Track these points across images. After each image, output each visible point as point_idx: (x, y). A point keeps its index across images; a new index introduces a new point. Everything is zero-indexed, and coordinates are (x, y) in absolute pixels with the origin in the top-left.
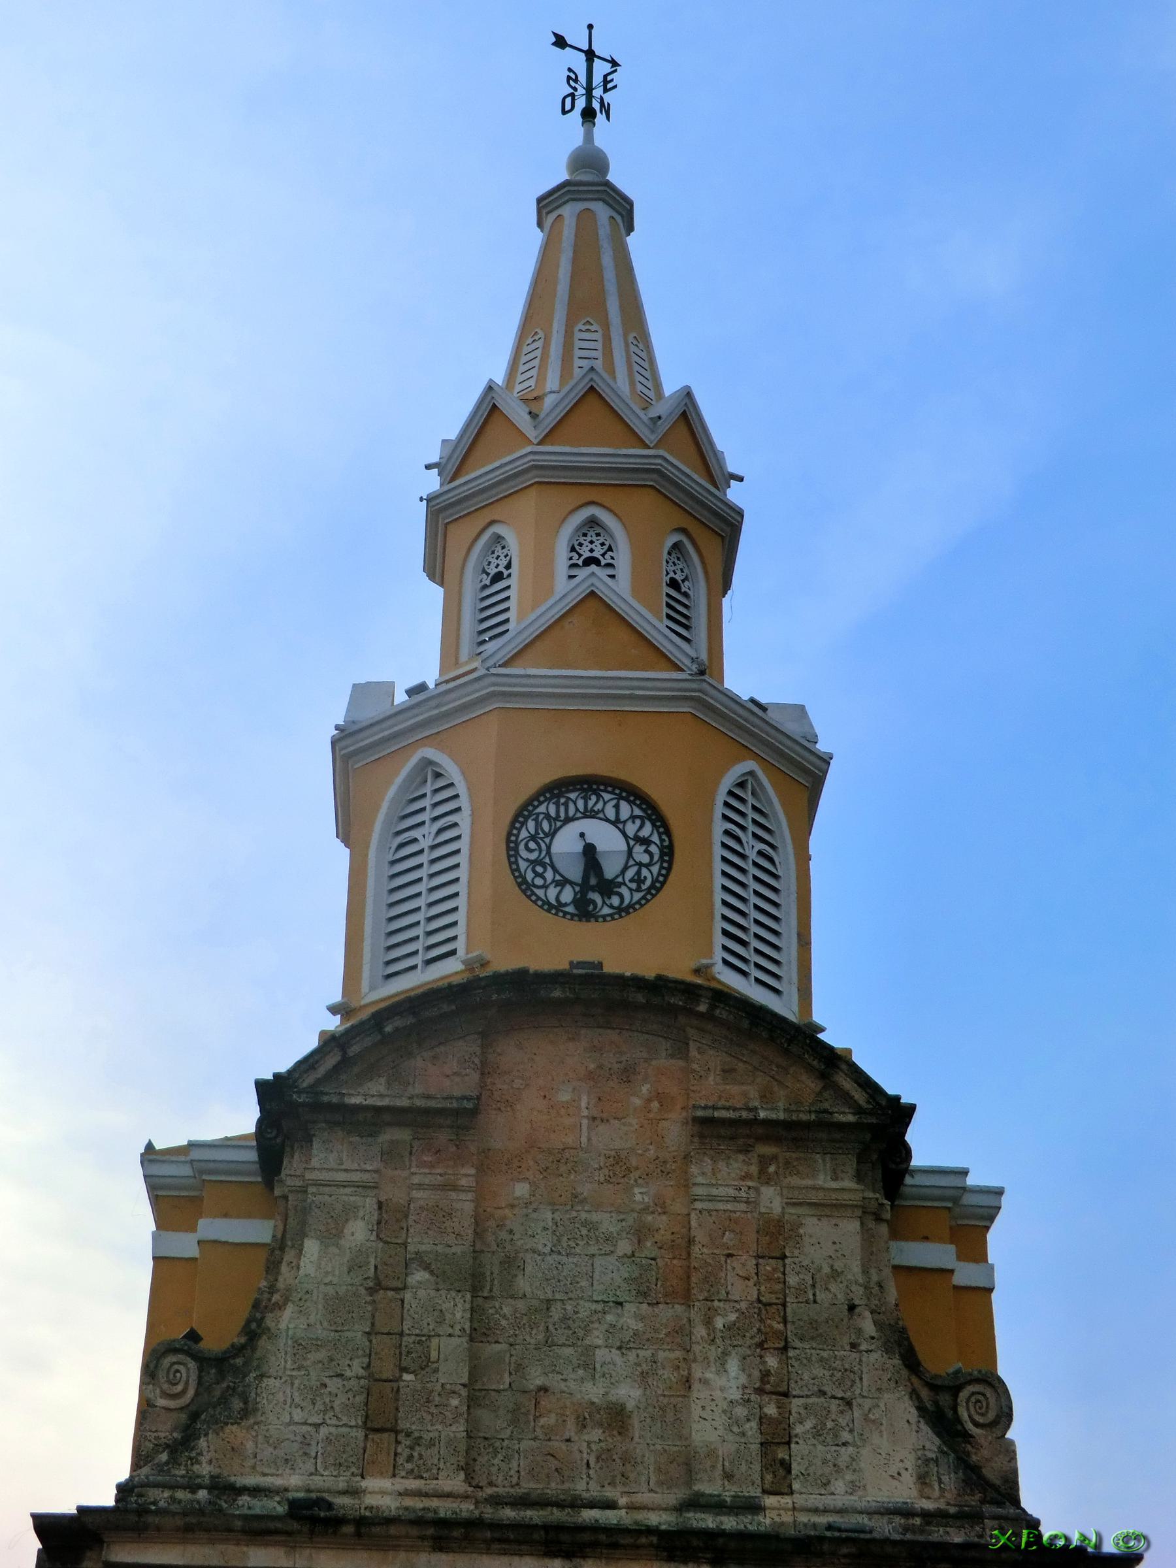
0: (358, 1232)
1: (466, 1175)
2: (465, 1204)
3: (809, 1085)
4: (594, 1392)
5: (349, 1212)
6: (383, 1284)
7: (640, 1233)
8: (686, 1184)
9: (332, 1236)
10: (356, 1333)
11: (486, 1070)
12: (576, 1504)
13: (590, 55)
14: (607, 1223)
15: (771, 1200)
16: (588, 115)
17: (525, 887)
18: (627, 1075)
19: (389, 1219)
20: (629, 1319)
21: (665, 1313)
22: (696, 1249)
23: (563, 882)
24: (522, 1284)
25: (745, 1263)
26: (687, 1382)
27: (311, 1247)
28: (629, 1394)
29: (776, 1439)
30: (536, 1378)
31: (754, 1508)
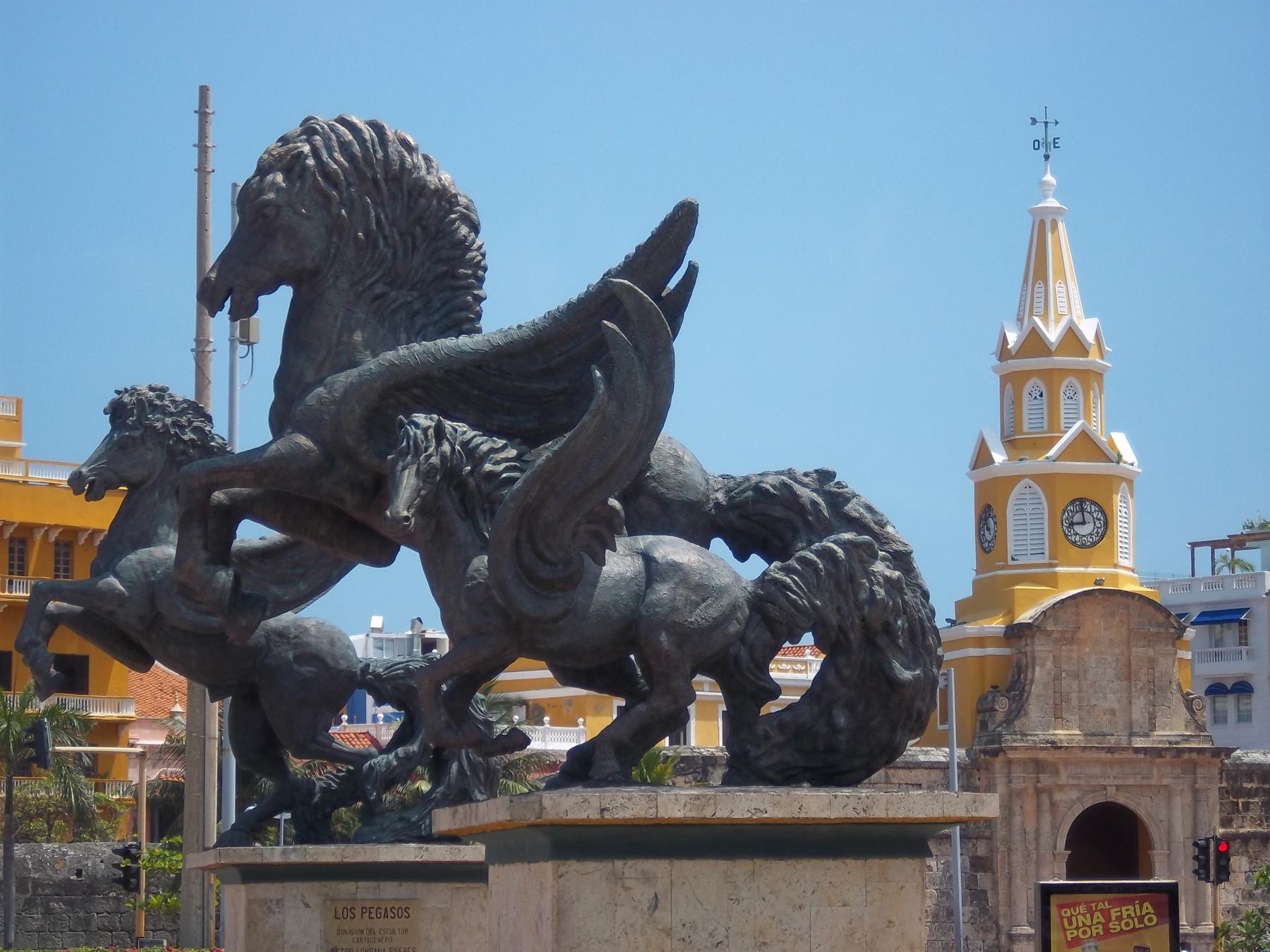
0: (1049, 664)
1: (1075, 647)
2: (1075, 656)
3: (1161, 618)
4: (1107, 705)
5: (1046, 658)
6: (1057, 678)
7: (1117, 661)
8: (1129, 648)
9: (1043, 665)
10: (1051, 692)
11: (1078, 614)
12: (1105, 735)
13: (1046, 123)
14: (1109, 658)
15: (1151, 652)
16: (1047, 157)
17: (1066, 536)
18: (1113, 615)
19: (1056, 660)
20: (1116, 685)
21: (1125, 683)
22: (1133, 668)
23: (1076, 534)
24: (1089, 676)
25: (1144, 670)
26: (1130, 702)
27: (1037, 669)
28: (1116, 706)
29: (1152, 717)
30: (1093, 702)
31: (1147, 735)
